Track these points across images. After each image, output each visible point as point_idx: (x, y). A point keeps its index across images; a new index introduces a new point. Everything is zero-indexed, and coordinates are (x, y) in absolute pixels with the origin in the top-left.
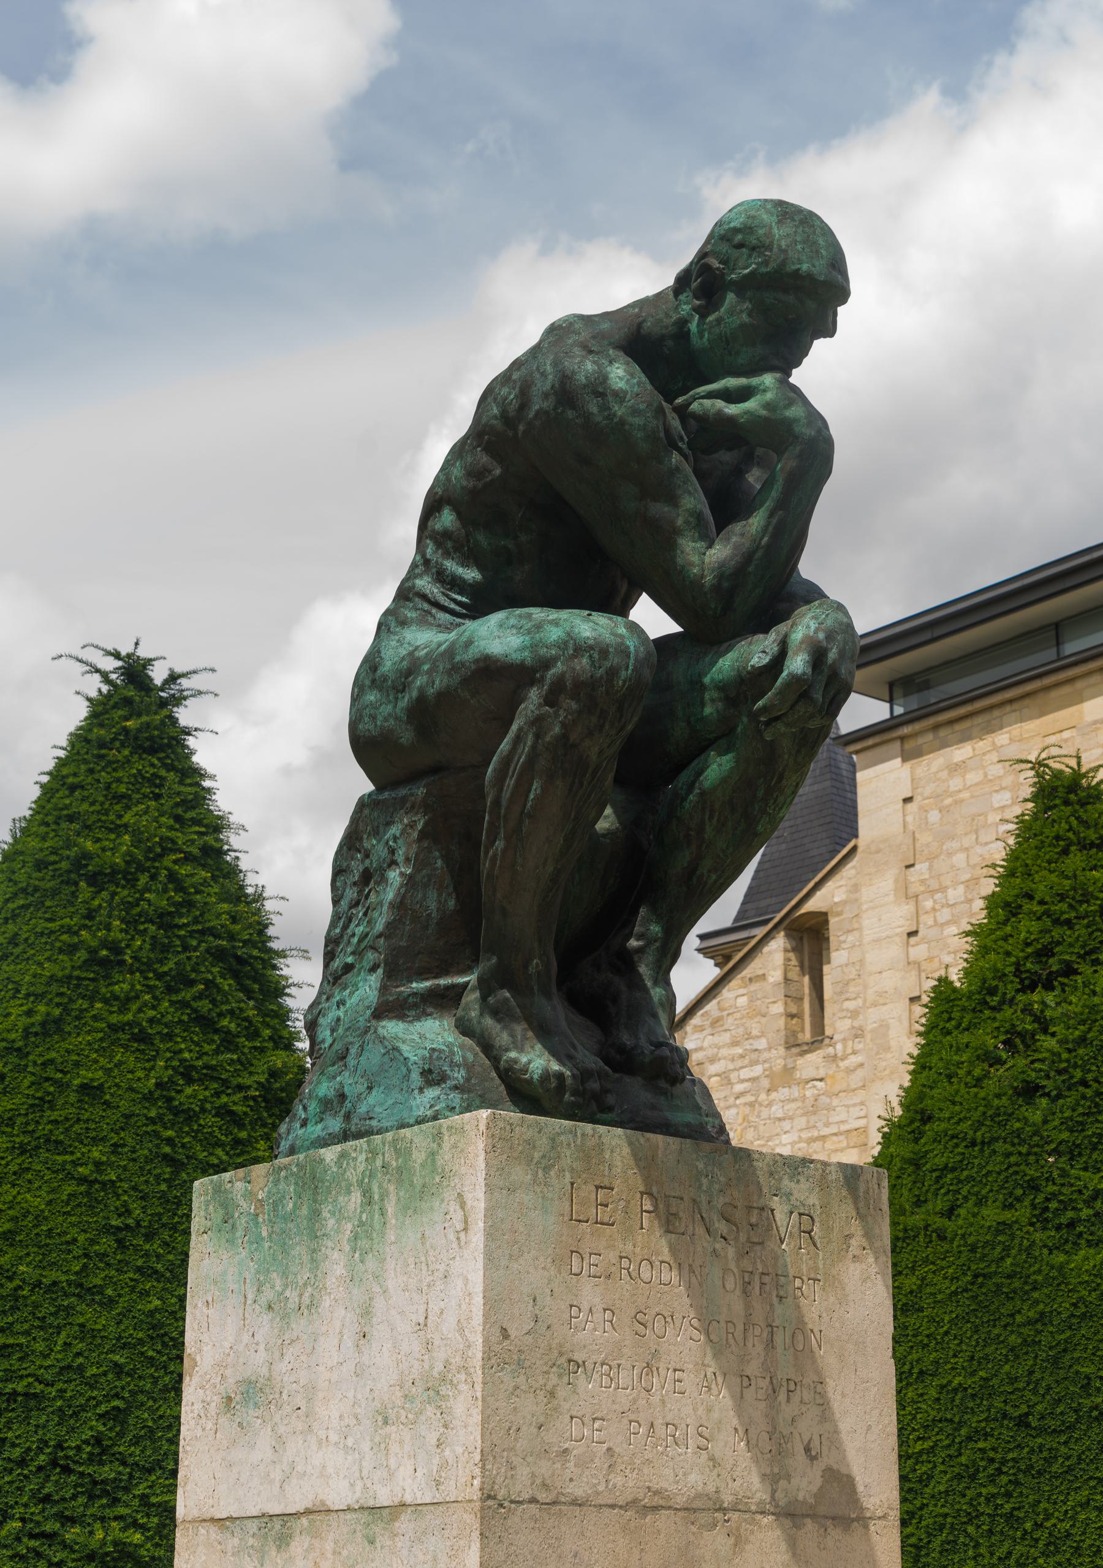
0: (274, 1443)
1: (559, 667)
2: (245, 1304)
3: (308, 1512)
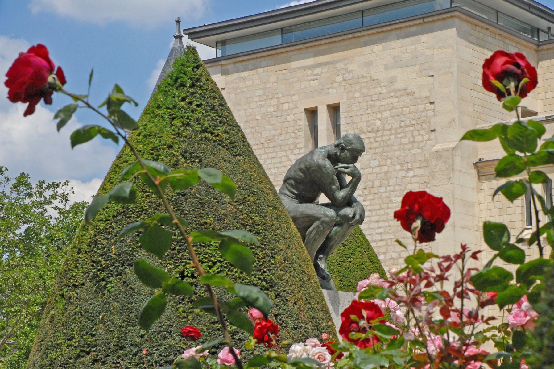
1: (323, 219)
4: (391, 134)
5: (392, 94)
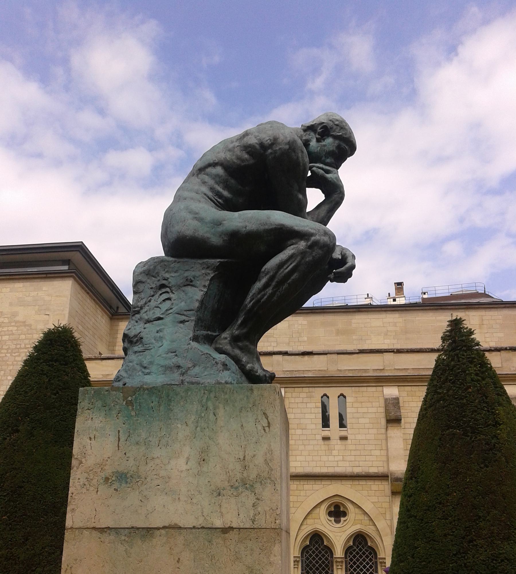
0: (140, 499)
1: (317, 237)
2: (119, 441)
3: (164, 528)
4: (7, 353)
5: (13, 324)
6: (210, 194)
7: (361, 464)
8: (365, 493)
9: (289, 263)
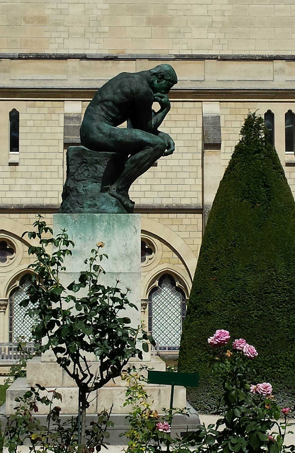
1: (158, 146)
6: (106, 116)
7: (172, 194)
8: (175, 228)
9: (145, 158)
